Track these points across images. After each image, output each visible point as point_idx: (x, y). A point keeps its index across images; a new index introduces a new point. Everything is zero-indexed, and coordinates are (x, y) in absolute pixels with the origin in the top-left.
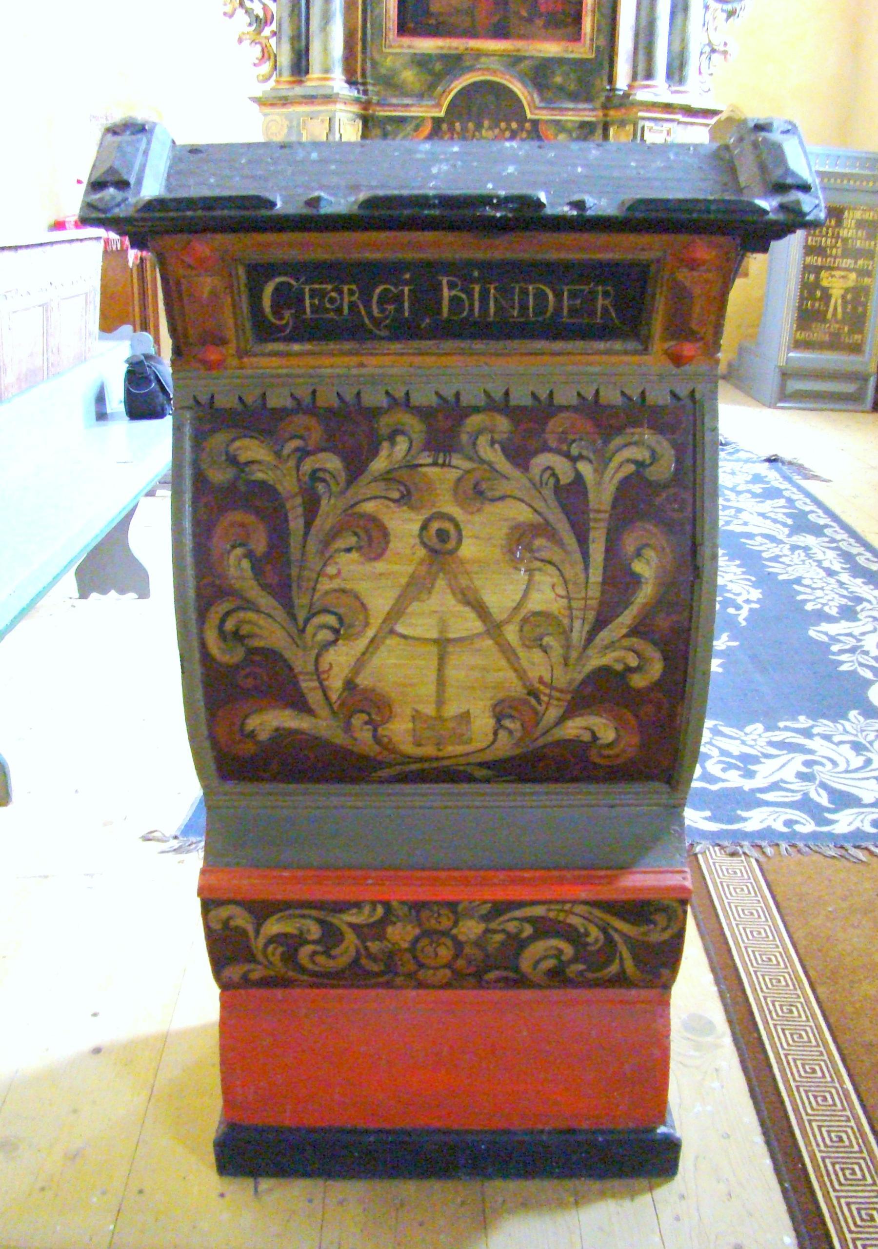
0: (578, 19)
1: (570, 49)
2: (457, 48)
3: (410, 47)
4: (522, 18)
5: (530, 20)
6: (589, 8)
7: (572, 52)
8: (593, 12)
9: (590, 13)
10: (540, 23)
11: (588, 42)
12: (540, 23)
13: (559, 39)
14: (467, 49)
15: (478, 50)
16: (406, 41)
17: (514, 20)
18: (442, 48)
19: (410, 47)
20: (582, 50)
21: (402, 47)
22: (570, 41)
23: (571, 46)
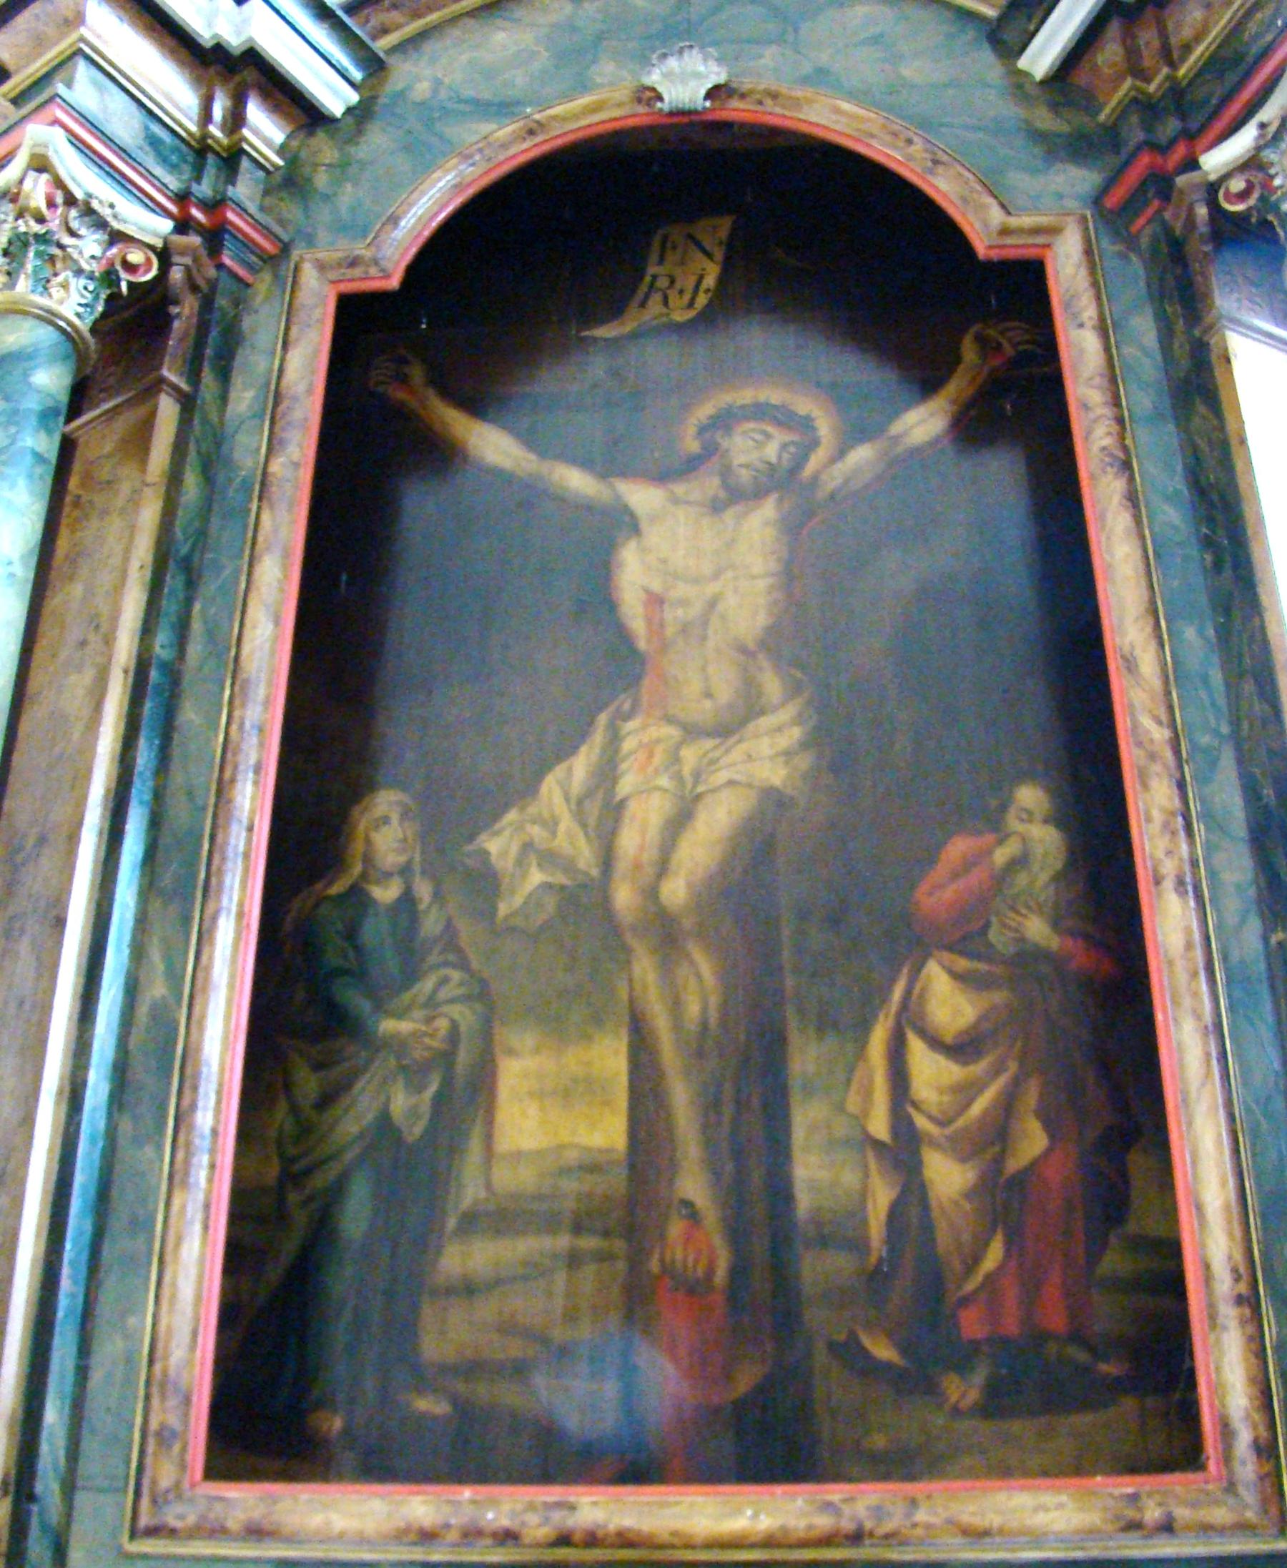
0: (1163, 1360)
1: (1152, 1514)
2: (508, 1537)
3: (256, 1532)
4: (868, 1368)
5: (916, 1381)
6: (1224, 1285)
7: (1167, 1527)
8: (1249, 1301)
9: (1229, 1314)
10: (963, 1389)
11: (1247, 1468)
12: (963, 1389)
13: (1076, 1466)
14: (564, 1540)
15: (625, 1540)
16: (243, 1500)
17: (832, 1386)
18: (427, 1536)
19: (256, 1532)
20: (1220, 1515)
21: (217, 1532)
22: (1133, 1468)
23: (1161, 1495)
